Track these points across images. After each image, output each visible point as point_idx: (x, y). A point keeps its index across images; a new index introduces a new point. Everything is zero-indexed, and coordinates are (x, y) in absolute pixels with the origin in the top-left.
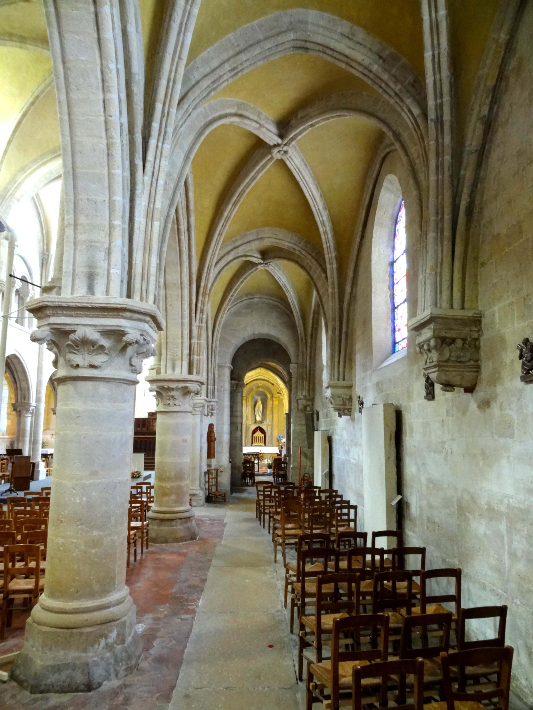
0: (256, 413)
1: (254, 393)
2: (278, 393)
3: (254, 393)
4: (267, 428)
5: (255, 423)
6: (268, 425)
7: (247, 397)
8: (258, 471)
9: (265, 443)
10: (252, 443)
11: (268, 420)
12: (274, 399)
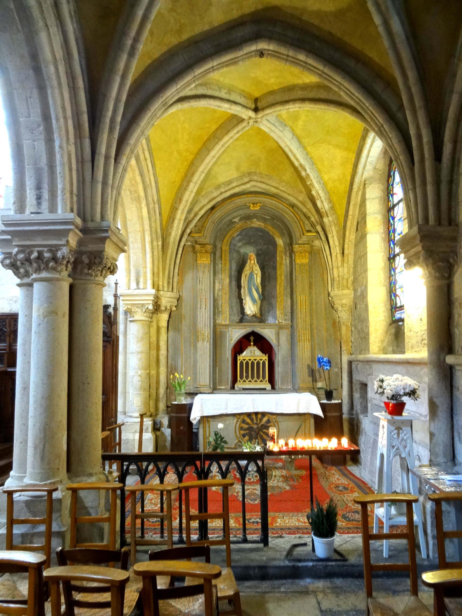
1: (234, 233)
2: (309, 231)
3: (234, 233)
4: (278, 334)
5: (241, 321)
6: (280, 327)
7: (215, 246)
8: (265, 540)
9: (272, 380)
10: (235, 380)
11: (278, 313)
12: (296, 248)
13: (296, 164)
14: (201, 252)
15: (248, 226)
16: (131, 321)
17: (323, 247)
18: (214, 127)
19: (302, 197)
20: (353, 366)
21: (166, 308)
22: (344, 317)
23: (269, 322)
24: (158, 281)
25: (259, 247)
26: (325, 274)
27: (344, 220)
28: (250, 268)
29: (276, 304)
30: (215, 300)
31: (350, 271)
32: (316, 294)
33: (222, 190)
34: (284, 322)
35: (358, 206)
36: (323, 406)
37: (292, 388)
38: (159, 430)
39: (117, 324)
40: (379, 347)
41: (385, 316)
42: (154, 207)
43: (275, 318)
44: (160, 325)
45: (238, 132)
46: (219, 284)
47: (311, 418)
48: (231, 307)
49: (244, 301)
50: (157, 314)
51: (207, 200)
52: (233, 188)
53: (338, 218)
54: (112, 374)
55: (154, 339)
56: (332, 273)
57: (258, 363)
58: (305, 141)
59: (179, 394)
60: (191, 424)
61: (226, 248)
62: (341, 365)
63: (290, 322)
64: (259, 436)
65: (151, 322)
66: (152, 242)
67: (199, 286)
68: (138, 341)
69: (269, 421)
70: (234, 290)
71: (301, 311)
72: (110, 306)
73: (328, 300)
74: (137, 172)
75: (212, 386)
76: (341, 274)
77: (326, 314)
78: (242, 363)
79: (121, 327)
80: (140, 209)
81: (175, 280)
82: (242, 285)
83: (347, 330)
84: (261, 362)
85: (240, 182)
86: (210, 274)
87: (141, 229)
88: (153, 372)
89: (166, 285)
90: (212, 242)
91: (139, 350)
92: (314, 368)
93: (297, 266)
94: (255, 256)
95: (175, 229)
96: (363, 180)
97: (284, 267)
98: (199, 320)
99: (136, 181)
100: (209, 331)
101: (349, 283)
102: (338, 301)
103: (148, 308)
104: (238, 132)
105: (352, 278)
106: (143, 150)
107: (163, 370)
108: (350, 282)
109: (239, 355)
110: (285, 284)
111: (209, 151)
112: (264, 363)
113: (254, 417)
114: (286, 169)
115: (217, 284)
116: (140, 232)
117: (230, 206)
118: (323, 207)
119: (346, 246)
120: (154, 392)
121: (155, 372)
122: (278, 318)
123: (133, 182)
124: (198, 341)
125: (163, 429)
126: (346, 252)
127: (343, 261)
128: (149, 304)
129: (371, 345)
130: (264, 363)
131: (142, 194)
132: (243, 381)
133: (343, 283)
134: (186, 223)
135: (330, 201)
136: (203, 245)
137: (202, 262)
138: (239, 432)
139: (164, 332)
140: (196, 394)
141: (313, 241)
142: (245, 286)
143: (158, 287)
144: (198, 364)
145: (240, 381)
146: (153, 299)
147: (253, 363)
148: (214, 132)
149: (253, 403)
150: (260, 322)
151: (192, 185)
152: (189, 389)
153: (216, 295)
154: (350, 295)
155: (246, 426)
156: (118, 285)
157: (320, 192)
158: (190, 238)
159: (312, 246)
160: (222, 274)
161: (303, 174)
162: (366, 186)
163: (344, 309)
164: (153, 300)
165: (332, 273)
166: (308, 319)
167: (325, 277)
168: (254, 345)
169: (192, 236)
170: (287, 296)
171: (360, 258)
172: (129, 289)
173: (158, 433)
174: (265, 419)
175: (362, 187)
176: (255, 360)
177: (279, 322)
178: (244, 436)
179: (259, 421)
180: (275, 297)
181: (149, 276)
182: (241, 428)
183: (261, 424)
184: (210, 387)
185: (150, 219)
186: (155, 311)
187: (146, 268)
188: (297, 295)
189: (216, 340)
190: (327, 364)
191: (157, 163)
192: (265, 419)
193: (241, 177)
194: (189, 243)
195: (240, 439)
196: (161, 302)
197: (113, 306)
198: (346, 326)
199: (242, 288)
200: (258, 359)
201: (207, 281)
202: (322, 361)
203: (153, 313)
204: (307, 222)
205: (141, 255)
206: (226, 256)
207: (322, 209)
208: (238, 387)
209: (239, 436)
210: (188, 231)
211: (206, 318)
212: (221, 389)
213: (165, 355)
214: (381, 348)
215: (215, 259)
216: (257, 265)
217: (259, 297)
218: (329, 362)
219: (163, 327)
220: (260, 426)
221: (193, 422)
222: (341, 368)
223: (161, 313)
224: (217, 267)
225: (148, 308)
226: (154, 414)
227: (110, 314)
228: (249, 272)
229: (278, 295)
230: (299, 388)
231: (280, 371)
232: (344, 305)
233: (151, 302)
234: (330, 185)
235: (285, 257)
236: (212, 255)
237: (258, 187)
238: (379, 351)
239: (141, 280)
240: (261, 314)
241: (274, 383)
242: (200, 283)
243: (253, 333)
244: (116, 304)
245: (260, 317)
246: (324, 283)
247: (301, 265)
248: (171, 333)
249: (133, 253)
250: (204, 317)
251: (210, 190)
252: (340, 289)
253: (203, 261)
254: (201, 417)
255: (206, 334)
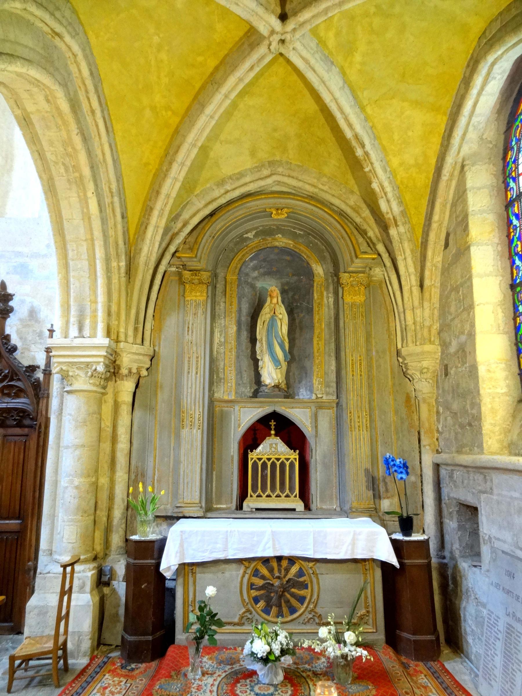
0: (261, 347)
5: (256, 394)
6: (320, 406)
7: (215, 276)
10: (243, 495)
11: (316, 382)
12: (345, 277)
13: (349, 134)
14: (191, 282)
15: (269, 245)
16: (68, 392)
17: (387, 278)
18: (212, 63)
19: (355, 199)
20: (443, 472)
21: (130, 372)
22: (425, 390)
23: (301, 397)
24: (118, 326)
25: (284, 280)
26: (391, 318)
27: (423, 232)
28: (271, 311)
29: (311, 368)
30: (213, 361)
31: (433, 314)
32: (377, 352)
33: (228, 187)
34: (324, 398)
35: (449, 206)
36: (395, 543)
37: (338, 509)
38: (107, 584)
39: (48, 397)
40: (500, 441)
41: (508, 386)
42: (112, 203)
43: (311, 391)
44: (120, 400)
45: (252, 68)
46: (221, 335)
47: (375, 567)
48: (239, 373)
49: (260, 363)
50: (116, 381)
51: (203, 203)
52: (246, 184)
53: (412, 230)
54: (35, 482)
55: (107, 423)
56: (402, 318)
57: (283, 465)
58: (365, 96)
59: (143, 522)
60: (162, 578)
61: (232, 277)
62: (421, 471)
63: (335, 397)
64: (282, 601)
65: (103, 394)
66: (107, 260)
67: (187, 337)
68: (76, 427)
69: (301, 573)
70: (244, 348)
71: (353, 380)
72: (38, 367)
73: (396, 362)
74: (73, 127)
75: (204, 505)
76: (418, 319)
77: (394, 384)
78: (255, 464)
79: (54, 403)
80: (84, 201)
81: (148, 326)
82: (258, 337)
83: (429, 411)
84: (288, 463)
85: (257, 175)
86: (206, 319)
87: (89, 237)
88: (104, 481)
89: (131, 333)
90: (210, 268)
91: (77, 441)
92: (376, 474)
93: (346, 306)
94: (278, 292)
95: (148, 241)
96: (460, 160)
97: (325, 310)
98: (185, 393)
99: (74, 148)
100: (201, 410)
101: (432, 334)
102: (414, 364)
103: (96, 369)
104: (252, 68)
105: (436, 326)
106: (87, 92)
107: (121, 476)
108: (434, 331)
109: (252, 451)
110: (327, 337)
111: (203, 106)
112: (292, 465)
113: (275, 564)
114: (329, 154)
115: (217, 335)
116: (86, 240)
117: (241, 212)
118: (389, 211)
119: (427, 273)
120: (102, 515)
121: (107, 479)
122: (315, 392)
123: (70, 149)
124: (183, 428)
125: (114, 583)
126: (427, 283)
127: (422, 299)
128: (98, 363)
129: (485, 439)
130: (292, 465)
131: (86, 171)
132: (257, 496)
133: (422, 334)
134: (168, 238)
135: (401, 203)
136: (195, 271)
137: (194, 298)
138: (248, 592)
139: (125, 412)
140: (178, 518)
141: (371, 269)
142: (262, 339)
143: (118, 337)
144: (182, 465)
145: (251, 496)
146: (105, 354)
147: (273, 465)
148: (212, 74)
149: (273, 541)
150: (286, 397)
151: (175, 167)
152: (165, 509)
153: (215, 353)
154: (435, 353)
155: (260, 582)
156: (54, 333)
157: (386, 184)
158: (175, 261)
159: (369, 276)
160: (225, 317)
161: (359, 152)
162: (466, 168)
163: (425, 376)
164: (105, 356)
165: (402, 318)
166: (365, 391)
167: (392, 325)
168: (276, 435)
169: (179, 258)
170: (330, 355)
171: (456, 289)
172: (66, 337)
173: (106, 590)
174: (294, 570)
175: (456, 173)
176: (278, 459)
177: (317, 398)
178: (256, 600)
179: (283, 571)
180: (310, 356)
181: (101, 315)
182: (252, 586)
183: (287, 579)
184: (201, 507)
185: (104, 221)
186: (111, 376)
187: (96, 302)
188: (347, 354)
189: (213, 425)
190: (401, 470)
191: (118, 127)
192: (294, 570)
193: (259, 168)
194: (173, 269)
195: (249, 606)
196: (122, 361)
197: (43, 367)
198: (429, 404)
199: (258, 342)
200: (283, 457)
201: (201, 330)
202: (392, 463)
203: (107, 379)
204: (361, 240)
205: (88, 280)
206: (233, 291)
207: (388, 213)
208: (248, 506)
209: (247, 601)
210: (172, 249)
211: (198, 389)
212: (220, 509)
213: (126, 451)
214: (505, 444)
215: (214, 295)
216: (283, 306)
217: (285, 356)
218: (405, 466)
219: (124, 403)
220: (285, 583)
221: (165, 574)
222: (421, 476)
223: (122, 380)
224: (217, 308)
225: (96, 369)
226: (101, 555)
227: (38, 380)
228: (268, 316)
229: (316, 354)
230: (351, 508)
231: (318, 479)
232: (425, 370)
233: (102, 360)
234: (402, 174)
235: (328, 294)
236: (210, 288)
237: (285, 184)
238: (502, 450)
239: (87, 322)
240: (288, 385)
241: (309, 499)
242: (188, 331)
243: (275, 415)
244: (48, 364)
245: (286, 389)
246: (390, 335)
247: (353, 305)
248: (137, 413)
249: (74, 277)
250: (194, 386)
251: (208, 185)
252: (418, 343)
253: (196, 296)
254: (179, 565)
255: (197, 416)
